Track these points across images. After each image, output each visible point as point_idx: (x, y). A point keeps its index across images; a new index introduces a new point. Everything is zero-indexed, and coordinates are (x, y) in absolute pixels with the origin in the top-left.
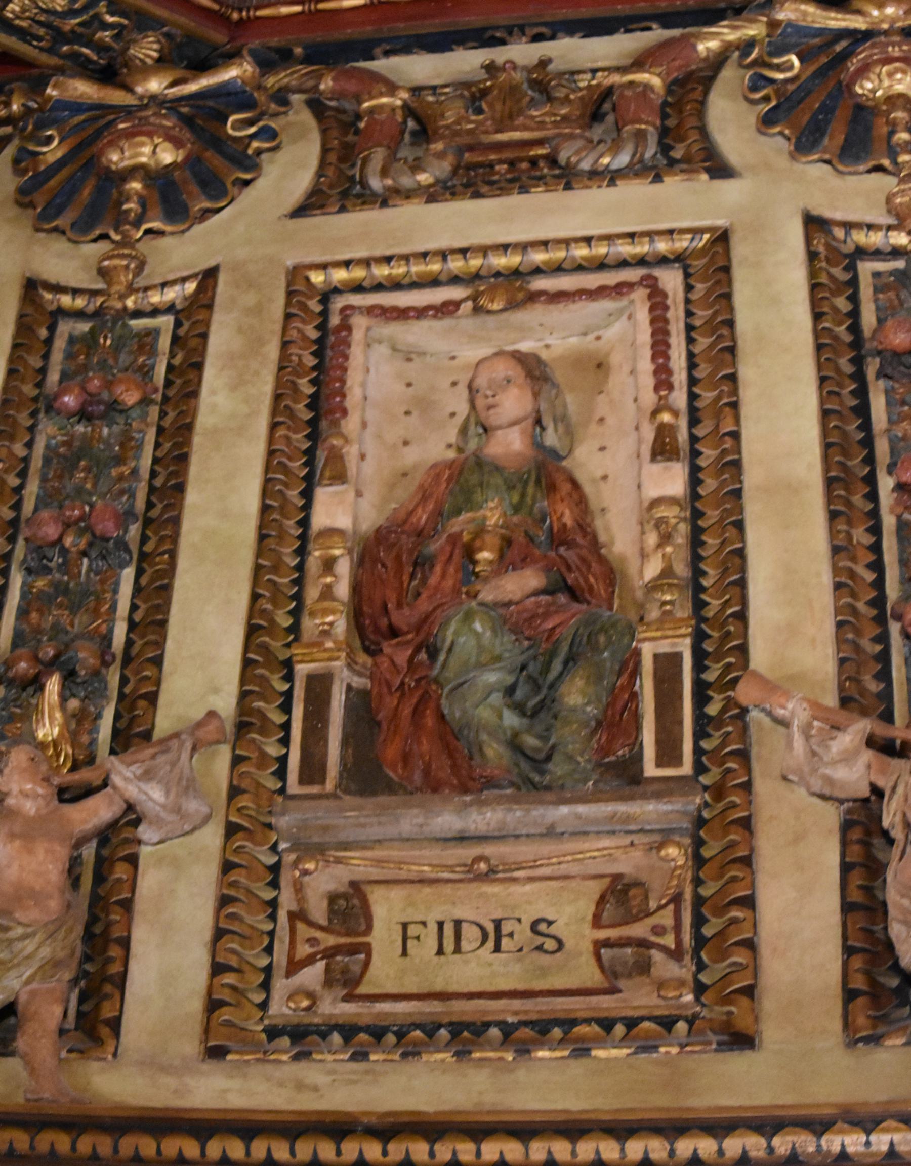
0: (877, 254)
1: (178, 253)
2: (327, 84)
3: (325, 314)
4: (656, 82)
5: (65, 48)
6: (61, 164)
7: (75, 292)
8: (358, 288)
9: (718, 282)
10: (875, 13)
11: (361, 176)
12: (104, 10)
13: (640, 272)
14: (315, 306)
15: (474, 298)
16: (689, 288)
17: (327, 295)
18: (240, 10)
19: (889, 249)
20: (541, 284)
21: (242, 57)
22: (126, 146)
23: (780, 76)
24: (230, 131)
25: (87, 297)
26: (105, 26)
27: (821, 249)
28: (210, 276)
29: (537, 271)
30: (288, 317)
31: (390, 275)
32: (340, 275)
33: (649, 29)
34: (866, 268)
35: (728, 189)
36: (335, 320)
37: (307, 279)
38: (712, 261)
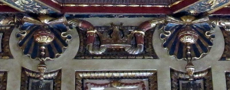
0: (183, 79)
1: (54, 64)
2: (80, 25)
3: (83, 84)
4: (143, 33)
5: (27, 9)
6: (27, 37)
7: (33, 72)
8: (89, 78)
9: (155, 85)
10: (184, 20)
11: (88, 49)
12: (36, 4)
13: (141, 80)
14: (80, 81)
15: (111, 83)
16: (149, 85)
17: (83, 79)
18: (63, 4)
19: (185, 78)
20: (123, 81)
21: (64, 17)
22: (41, 38)
23: (167, 35)
24: (62, 36)
25: (35, 74)
26: (36, 7)
27: (173, 78)
28: (60, 71)
29: (122, 78)
30: (76, 85)
31: (95, 76)
32: (85, 75)
33: (142, 17)
34: (181, 82)
35: (157, 61)
36: (85, 86)
37: (79, 76)
38: (153, 80)
